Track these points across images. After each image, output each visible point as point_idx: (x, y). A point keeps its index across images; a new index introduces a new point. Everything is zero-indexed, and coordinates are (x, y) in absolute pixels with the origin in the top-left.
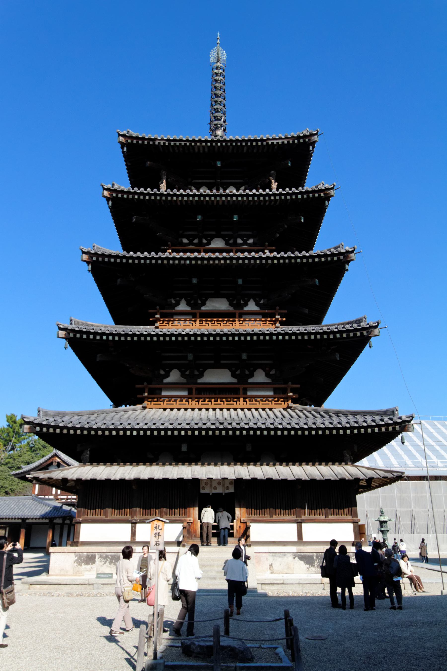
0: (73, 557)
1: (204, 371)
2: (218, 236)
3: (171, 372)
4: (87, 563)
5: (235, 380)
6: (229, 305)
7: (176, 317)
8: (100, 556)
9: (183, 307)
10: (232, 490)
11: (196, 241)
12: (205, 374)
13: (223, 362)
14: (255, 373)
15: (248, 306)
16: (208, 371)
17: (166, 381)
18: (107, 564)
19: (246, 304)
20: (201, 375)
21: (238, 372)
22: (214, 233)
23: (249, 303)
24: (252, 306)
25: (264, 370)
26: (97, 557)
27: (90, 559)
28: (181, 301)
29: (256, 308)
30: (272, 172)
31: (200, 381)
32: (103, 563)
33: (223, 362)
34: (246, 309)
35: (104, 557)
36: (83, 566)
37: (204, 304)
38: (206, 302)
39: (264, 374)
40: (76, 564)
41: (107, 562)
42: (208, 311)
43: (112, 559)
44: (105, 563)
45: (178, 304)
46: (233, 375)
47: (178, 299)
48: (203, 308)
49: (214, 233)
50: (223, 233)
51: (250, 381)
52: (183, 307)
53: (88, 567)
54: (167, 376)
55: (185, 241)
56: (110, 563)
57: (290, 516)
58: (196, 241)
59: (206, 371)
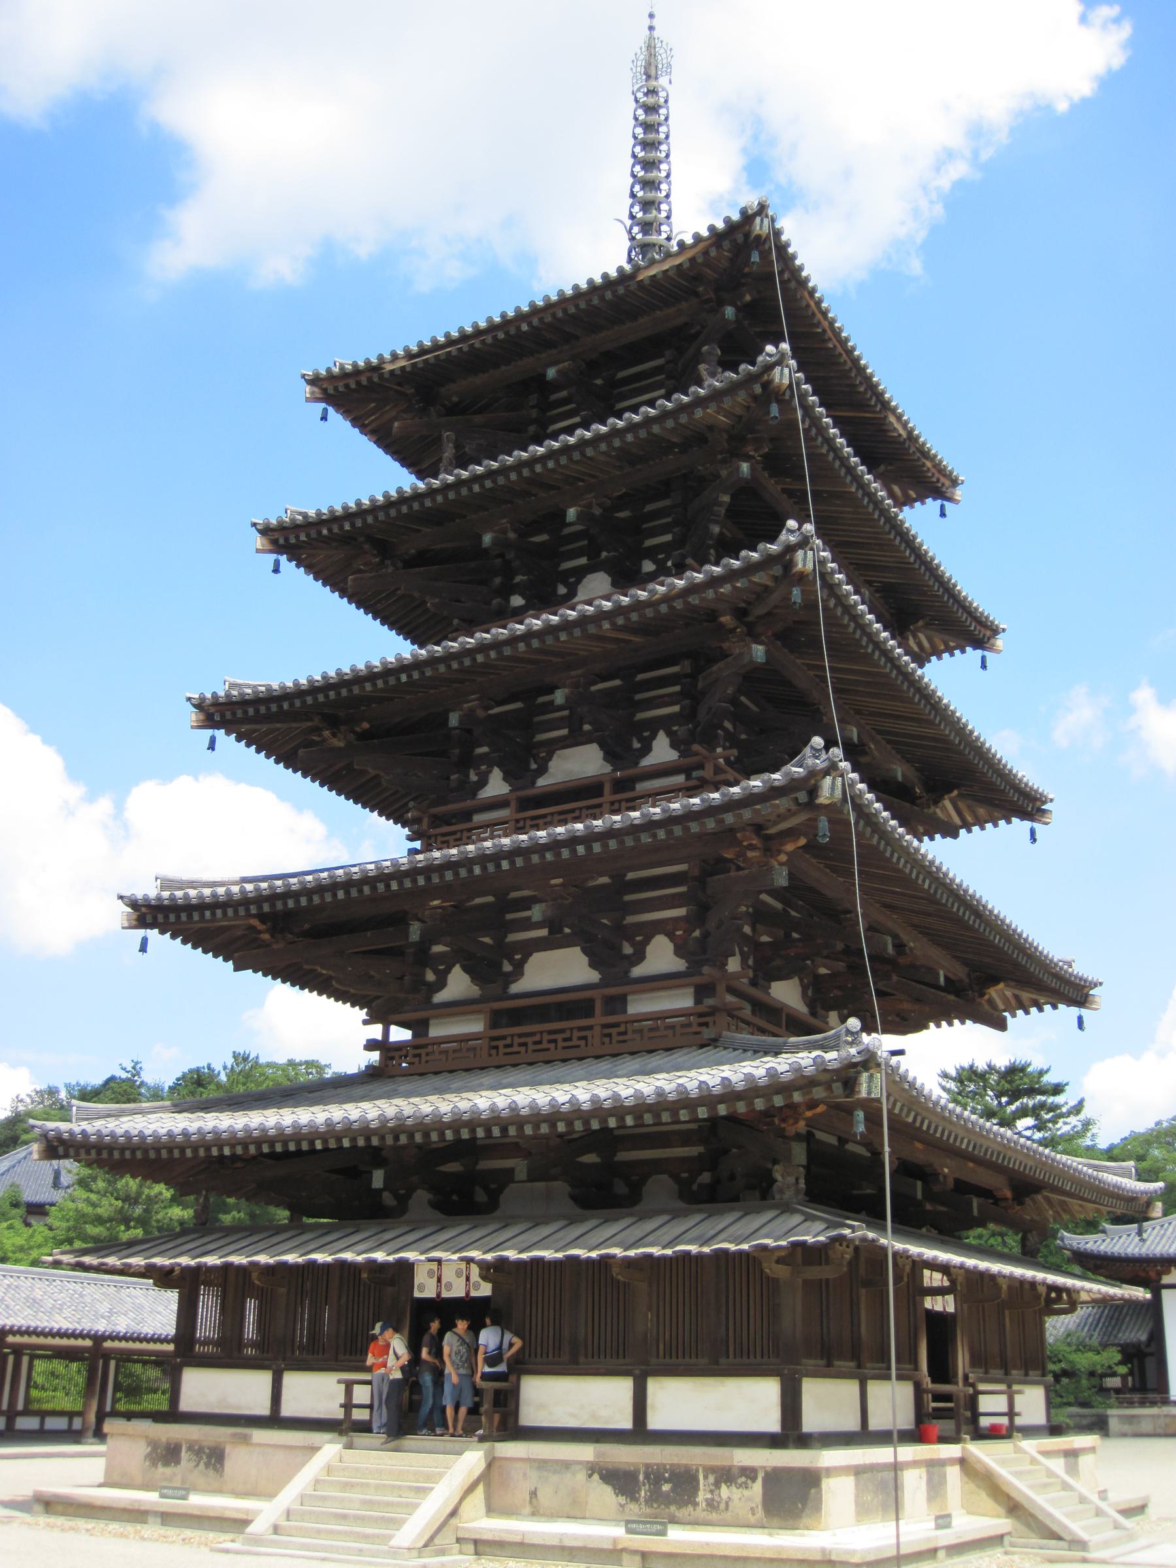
0: (141, 1449)
3: (449, 972)
4: (167, 1464)
5: (593, 976)
6: (605, 759)
7: (478, 818)
8: (190, 1449)
12: (529, 967)
14: (649, 949)
15: (652, 754)
16: (537, 958)
17: (440, 997)
18: (202, 1465)
19: (647, 749)
22: (583, 561)
23: (655, 743)
24: (662, 751)
25: (671, 936)
26: (184, 1449)
27: (169, 1454)
28: (491, 772)
29: (671, 755)
30: (705, 348)
31: (515, 988)
32: (194, 1464)
34: (647, 762)
35: (197, 1450)
36: (161, 1469)
37: (543, 770)
38: (551, 764)
39: (671, 946)
40: (147, 1463)
41: (202, 1465)
42: (555, 787)
43: (209, 1457)
44: (197, 1465)
45: (483, 782)
47: (484, 767)
48: (541, 782)
49: (583, 561)
51: (637, 971)
52: (496, 786)
53: (168, 1471)
54: (441, 984)
56: (207, 1465)
57: (621, 1361)
59: (531, 959)
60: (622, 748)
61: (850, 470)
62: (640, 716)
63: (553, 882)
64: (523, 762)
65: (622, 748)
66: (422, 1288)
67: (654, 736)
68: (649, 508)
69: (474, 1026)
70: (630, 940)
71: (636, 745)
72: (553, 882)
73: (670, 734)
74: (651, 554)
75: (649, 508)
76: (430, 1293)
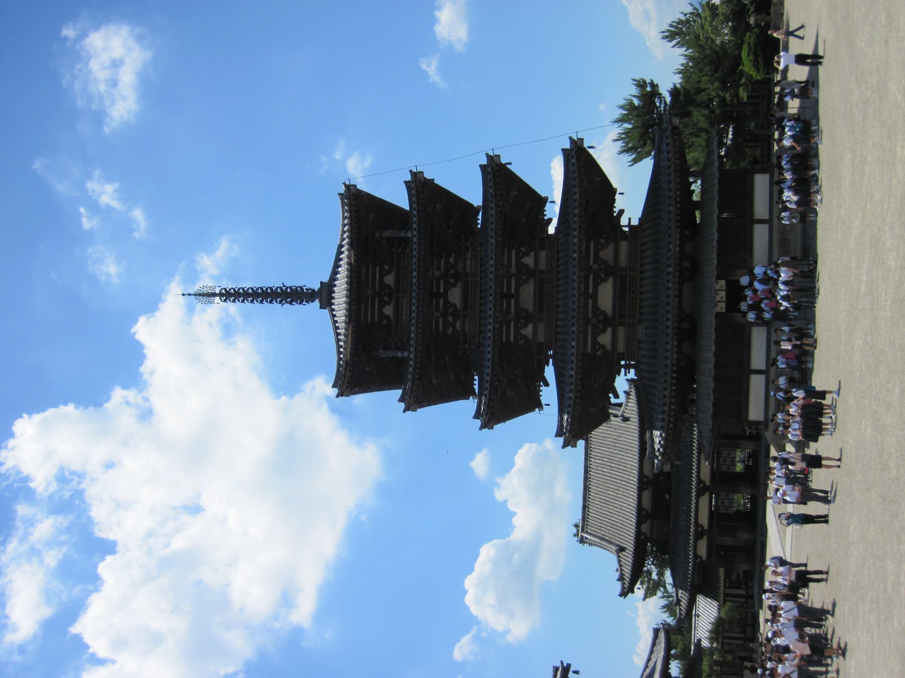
1: (599, 310)
2: (445, 296)
10: (723, 283)
11: (450, 319)
13: (591, 291)
20: (604, 313)
21: (603, 276)
22: (441, 301)
25: (601, 250)
33: (591, 291)
45: (525, 337)
46: (604, 280)
49: (441, 301)
50: (442, 291)
55: (450, 331)
58: (450, 319)
66: (722, 309)
67: (522, 263)
69: (621, 331)
73: (522, 257)
76: (723, 305)
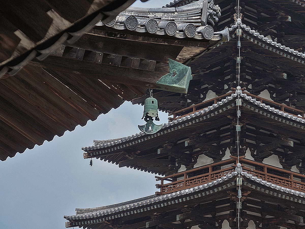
9: (183, 169)
19: (224, 154)
24: (228, 156)
37: (195, 162)
45: (179, 167)
52: (183, 169)
60: (216, 155)
61: (283, 51)
62: (222, 142)
63: (185, 206)
64: (189, 161)
65: (216, 155)
68: (226, 65)
70: (217, 221)
71: (221, 153)
72: (185, 206)
74: (227, 82)
75: (226, 65)
